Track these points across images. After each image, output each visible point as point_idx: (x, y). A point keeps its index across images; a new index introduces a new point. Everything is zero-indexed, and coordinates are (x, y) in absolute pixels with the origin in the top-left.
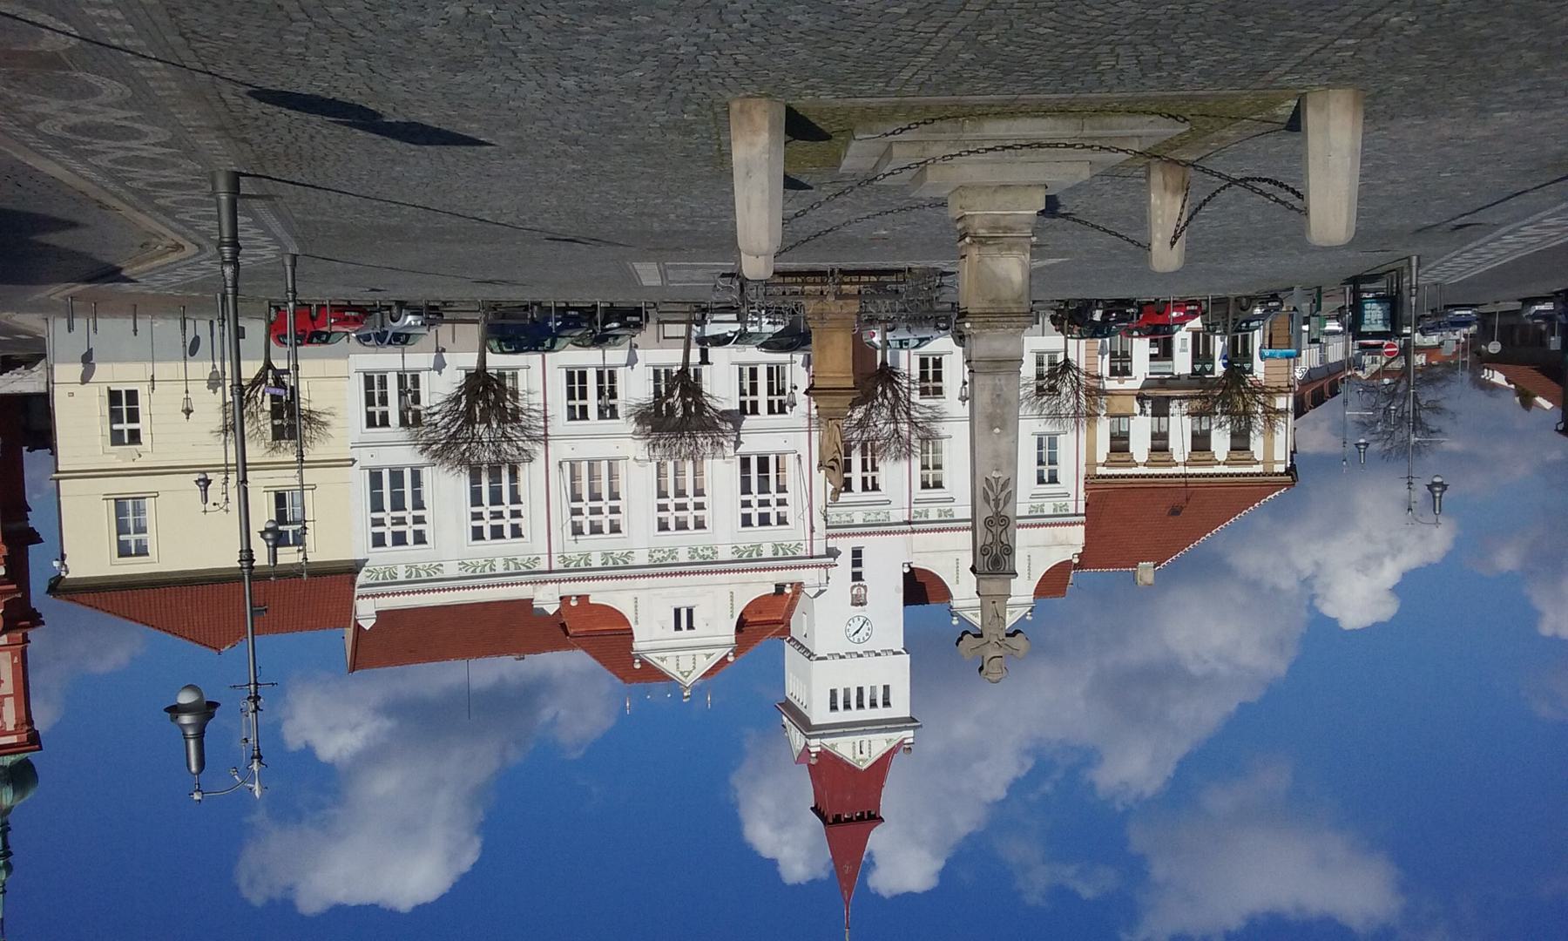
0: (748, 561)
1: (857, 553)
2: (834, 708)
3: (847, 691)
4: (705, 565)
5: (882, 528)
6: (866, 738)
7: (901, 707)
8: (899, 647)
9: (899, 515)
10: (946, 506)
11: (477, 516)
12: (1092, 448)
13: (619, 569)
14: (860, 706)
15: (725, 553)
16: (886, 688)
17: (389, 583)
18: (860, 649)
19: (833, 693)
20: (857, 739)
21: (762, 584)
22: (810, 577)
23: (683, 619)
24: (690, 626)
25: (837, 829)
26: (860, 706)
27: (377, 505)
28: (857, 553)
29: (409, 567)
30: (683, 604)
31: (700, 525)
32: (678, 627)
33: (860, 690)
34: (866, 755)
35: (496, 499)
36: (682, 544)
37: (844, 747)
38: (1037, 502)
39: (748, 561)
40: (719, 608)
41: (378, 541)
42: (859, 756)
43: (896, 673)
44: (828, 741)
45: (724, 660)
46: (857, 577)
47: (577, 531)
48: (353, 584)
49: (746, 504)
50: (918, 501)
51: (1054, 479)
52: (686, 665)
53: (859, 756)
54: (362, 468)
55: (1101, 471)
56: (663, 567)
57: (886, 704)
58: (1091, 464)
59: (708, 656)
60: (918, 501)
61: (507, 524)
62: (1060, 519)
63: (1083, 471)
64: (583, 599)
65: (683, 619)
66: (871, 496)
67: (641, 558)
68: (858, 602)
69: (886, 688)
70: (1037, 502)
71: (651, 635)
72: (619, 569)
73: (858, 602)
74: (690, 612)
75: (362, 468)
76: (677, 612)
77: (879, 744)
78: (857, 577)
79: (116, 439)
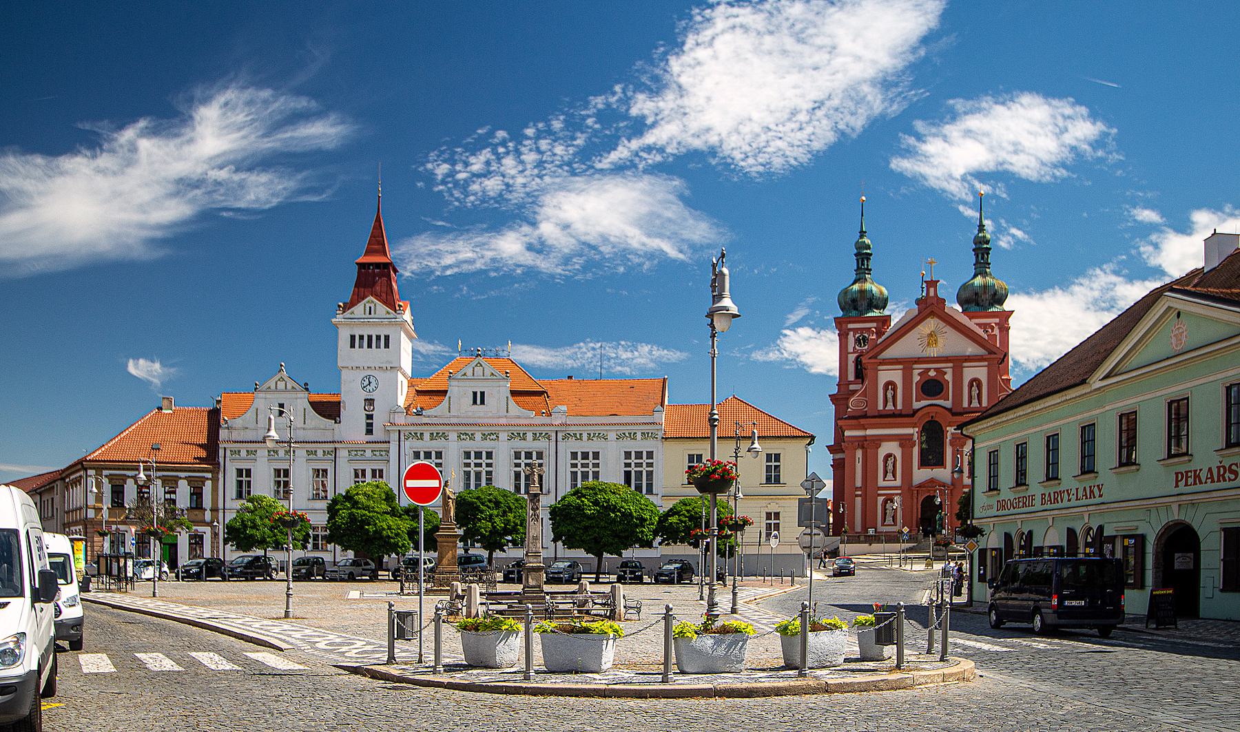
1: (369, 431)
3: (361, 346)
8: (344, 372)
11: (596, 465)
14: (370, 337)
16: (353, 346)
19: (387, 346)
23: (479, 398)
26: (370, 337)
27: (650, 474)
28: (369, 431)
30: (478, 408)
32: (482, 394)
33: (370, 346)
35: (478, 475)
36: (478, 444)
46: (370, 417)
47: (540, 455)
49: (489, 465)
55: (209, 475)
57: (353, 337)
58: (215, 480)
61: (633, 461)
63: (221, 476)
65: (479, 398)
66: (360, 466)
69: (353, 346)
73: (370, 402)
74: (475, 402)
76: (482, 402)
78: (370, 417)
79: (777, 515)
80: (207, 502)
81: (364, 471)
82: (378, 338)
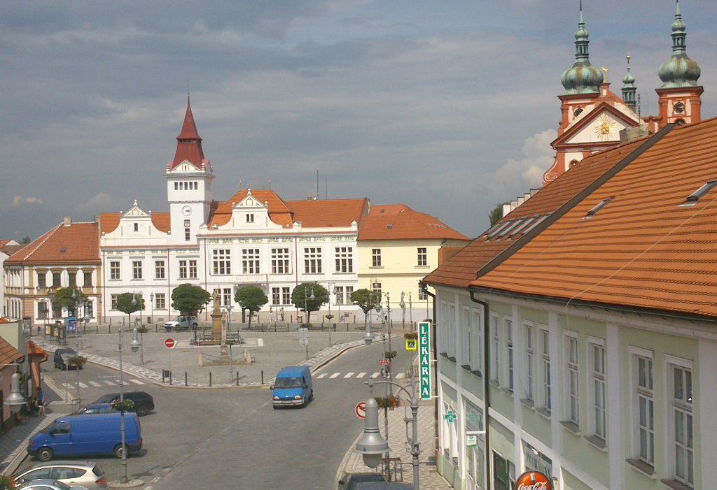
0: (228, 238)
1: (188, 238)
2: (196, 183)
4: (243, 237)
5: (179, 248)
6: (184, 171)
7: (171, 184)
8: (172, 205)
9: (173, 253)
10: (155, 254)
12: (99, 275)
13: (273, 237)
15: (236, 241)
17: (348, 235)
18: (187, 204)
19: (196, 188)
20: (187, 171)
21: (223, 229)
22: (205, 231)
23: (250, 218)
24: (248, 215)
25: (196, 137)
28: (188, 238)
29: (341, 240)
30: (250, 224)
31: (245, 251)
32: (252, 215)
34: (184, 165)
36: (251, 245)
37: (192, 169)
38: (120, 255)
39: (228, 238)
40: (238, 223)
41: (350, 249)
42: (187, 165)
43: (173, 194)
44: (198, 171)
45: (236, 203)
46: (187, 230)
48: (359, 236)
50: (166, 257)
51: (113, 264)
52: (249, 202)
53: (187, 165)
54: (355, 274)
55: (95, 267)
56: (257, 237)
57: (176, 184)
58: (99, 270)
59: (242, 205)
60: (166, 257)
62: (110, 249)
63: (102, 267)
64: (285, 227)
65: (250, 218)
67: (265, 241)
68: (187, 221)
69: (176, 189)
70: (120, 255)
71: (262, 215)
72: (273, 237)
73: (187, 221)
74: (248, 220)
75: (355, 274)
77: (179, 169)
78: (187, 230)
80: (94, 282)
81: (185, 262)
82: (191, 183)
